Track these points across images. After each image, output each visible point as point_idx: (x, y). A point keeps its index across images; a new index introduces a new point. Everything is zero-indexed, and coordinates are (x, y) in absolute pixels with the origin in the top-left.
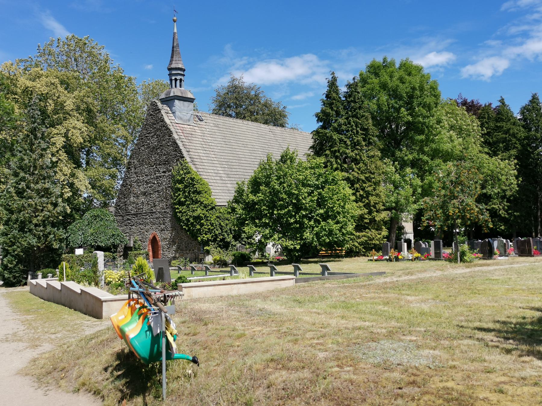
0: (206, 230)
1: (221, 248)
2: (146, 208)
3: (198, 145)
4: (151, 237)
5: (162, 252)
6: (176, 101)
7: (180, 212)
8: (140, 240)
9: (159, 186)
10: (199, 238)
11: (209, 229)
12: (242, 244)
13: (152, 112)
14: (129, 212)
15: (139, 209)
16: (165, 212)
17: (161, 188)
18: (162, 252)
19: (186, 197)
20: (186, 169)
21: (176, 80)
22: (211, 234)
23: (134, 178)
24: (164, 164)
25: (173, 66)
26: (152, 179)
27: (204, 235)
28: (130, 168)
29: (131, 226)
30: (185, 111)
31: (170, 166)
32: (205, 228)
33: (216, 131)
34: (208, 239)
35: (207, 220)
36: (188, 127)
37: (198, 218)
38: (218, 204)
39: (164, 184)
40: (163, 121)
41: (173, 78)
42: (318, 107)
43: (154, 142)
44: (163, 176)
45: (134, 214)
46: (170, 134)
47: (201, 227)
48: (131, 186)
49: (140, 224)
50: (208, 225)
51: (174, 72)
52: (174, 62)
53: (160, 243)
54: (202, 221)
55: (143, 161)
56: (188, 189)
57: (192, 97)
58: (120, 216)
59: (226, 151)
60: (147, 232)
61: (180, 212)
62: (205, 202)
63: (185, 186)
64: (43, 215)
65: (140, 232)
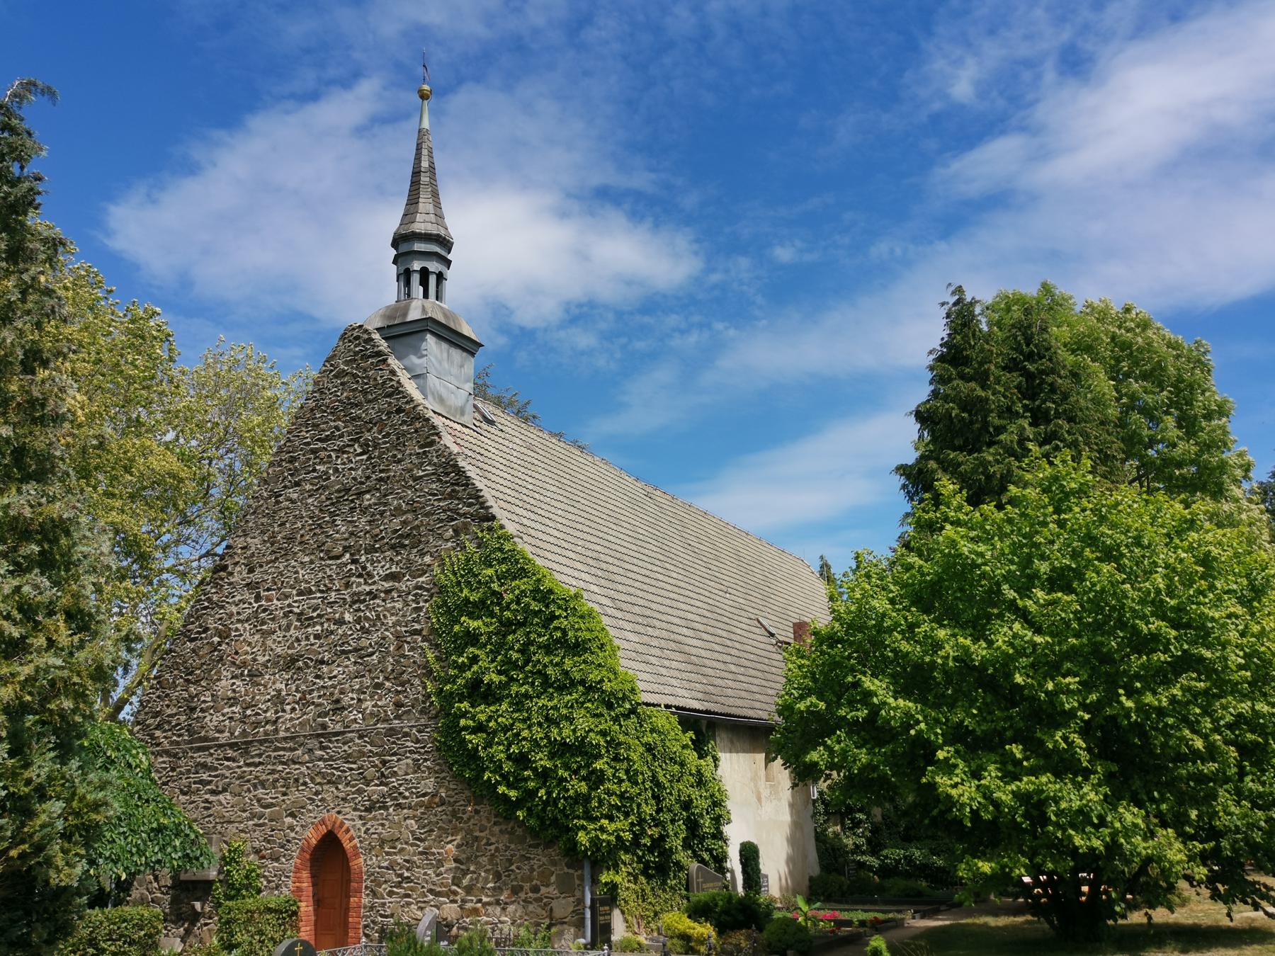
0: (614, 800)
1: (649, 877)
2: (290, 719)
3: (508, 491)
4: (312, 836)
5: (365, 900)
6: (429, 336)
7: (480, 728)
8: (257, 851)
9: (368, 632)
10: (582, 837)
11: (621, 796)
12: (702, 861)
13: (347, 363)
14: (206, 739)
15: (257, 724)
16: (391, 732)
17: (375, 637)
18: (365, 900)
19: (508, 667)
20: (502, 561)
21: (424, 273)
22: (627, 815)
23: (240, 603)
24: (393, 547)
25: (420, 227)
26: (331, 604)
27: (605, 822)
28: (224, 568)
29: (213, 792)
30: (452, 379)
31: (422, 555)
32: (609, 793)
33: (536, 462)
34: (619, 838)
35: (616, 758)
36: (465, 430)
37: (581, 749)
38: (645, 698)
39: (391, 620)
40: (398, 390)
41: (417, 265)
42: (921, 393)
43: (352, 466)
44: (388, 592)
45: (232, 746)
46: (429, 436)
47: (594, 787)
48: (224, 635)
49: (263, 784)
50: (621, 781)
51: (419, 246)
52: (419, 217)
53: (360, 863)
54: (598, 765)
55: (290, 539)
56: (512, 634)
57: (473, 337)
58: (159, 754)
59: (579, 527)
60: (292, 815)
61: (480, 728)
62: (607, 686)
63: (509, 623)
64: (27, 670)
65: (253, 816)
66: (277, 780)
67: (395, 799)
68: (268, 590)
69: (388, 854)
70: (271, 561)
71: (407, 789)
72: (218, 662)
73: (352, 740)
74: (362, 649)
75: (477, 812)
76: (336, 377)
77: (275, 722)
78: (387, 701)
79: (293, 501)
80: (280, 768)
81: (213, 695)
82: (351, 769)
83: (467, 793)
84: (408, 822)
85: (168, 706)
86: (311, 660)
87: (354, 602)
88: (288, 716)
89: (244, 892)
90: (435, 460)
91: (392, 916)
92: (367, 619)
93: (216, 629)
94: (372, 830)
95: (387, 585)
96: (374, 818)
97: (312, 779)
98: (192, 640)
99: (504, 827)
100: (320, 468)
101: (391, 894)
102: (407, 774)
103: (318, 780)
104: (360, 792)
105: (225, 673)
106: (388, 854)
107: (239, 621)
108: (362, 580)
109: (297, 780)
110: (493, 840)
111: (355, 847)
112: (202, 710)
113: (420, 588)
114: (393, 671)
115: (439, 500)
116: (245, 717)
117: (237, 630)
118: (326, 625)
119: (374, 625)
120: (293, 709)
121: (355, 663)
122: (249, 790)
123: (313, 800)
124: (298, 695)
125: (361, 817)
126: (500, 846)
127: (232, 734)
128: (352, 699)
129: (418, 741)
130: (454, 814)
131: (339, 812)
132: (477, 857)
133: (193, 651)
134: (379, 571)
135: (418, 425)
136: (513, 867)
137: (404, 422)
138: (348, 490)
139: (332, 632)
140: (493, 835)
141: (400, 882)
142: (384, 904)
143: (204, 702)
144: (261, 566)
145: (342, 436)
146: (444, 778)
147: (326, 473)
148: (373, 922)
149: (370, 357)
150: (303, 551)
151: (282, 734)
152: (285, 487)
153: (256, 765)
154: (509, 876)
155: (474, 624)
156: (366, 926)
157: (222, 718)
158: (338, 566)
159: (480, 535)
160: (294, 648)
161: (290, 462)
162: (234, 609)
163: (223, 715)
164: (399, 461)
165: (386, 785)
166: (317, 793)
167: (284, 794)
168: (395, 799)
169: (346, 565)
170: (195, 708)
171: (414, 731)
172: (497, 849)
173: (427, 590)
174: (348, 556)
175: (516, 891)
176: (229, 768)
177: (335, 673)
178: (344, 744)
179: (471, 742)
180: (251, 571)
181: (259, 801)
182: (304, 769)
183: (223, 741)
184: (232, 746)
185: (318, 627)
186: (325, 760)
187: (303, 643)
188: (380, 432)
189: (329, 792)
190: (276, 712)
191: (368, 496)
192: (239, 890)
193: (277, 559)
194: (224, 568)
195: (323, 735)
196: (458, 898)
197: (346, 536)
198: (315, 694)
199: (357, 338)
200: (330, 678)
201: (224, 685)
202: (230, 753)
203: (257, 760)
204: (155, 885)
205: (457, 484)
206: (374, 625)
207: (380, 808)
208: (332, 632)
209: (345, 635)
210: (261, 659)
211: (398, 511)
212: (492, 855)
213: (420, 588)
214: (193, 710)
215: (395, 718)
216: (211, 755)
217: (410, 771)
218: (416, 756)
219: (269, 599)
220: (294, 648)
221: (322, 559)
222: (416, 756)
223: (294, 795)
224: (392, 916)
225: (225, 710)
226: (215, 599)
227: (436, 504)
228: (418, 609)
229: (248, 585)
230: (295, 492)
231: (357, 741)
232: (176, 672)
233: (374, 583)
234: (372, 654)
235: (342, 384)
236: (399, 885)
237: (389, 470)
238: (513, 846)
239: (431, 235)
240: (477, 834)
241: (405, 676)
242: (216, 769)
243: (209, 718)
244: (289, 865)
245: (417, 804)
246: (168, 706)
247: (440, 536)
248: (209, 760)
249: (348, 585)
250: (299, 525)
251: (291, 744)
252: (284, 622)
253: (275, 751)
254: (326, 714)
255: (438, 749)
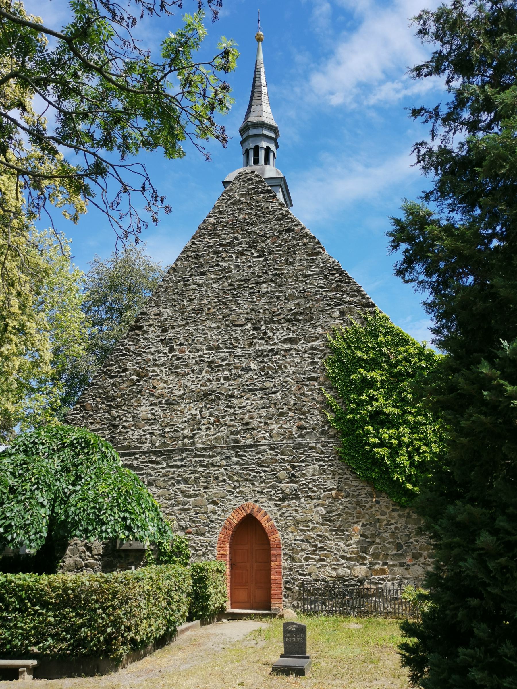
5: (285, 564)
8: (183, 529)
14: (128, 448)
15: (175, 439)
16: (299, 446)
24: (289, 321)
31: (315, 327)
39: (291, 370)
44: (287, 350)
45: (155, 453)
46: (315, 250)
49: (186, 481)
53: (278, 537)
55: (199, 310)
60: (214, 503)
65: (177, 504)
66: (199, 478)
67: (306, 492)
68: (181, 344)
69: (302, 530)
70: (182, 325)
71: (315, 486)
72: (138, 393)
73: (265, 451)
74: (267, 388)
75: (377, 502)
76: (232, 204)
77: (192, 437)
78: (291, 426)
79: (199, 285)
80: (201, 469)
81: (133, 417)
82: (265, 471)
83: (368, 489)
84: (319, 508)
85: (92, 423)
86: (223, 394)
87: (258, 357)
88: (204, 433)
89: (174, 558)
90: (322, 265)
91: (310, 574)
92: (270, 368)
93: (135, 370)
94: (287, 514)
95: (287, 346)
96: (289, 506)
97: (230, 478)
98: (111, 377)
99: (401, 513)
100: (224, 264)
101: (307, 559)
102: (314, 475)
103: (236, 478)
104: (273, 487)
105: (144, 401)
106: (302, 530)
107: (155, 365)
108: (263, 342)
109: (217, 478)
110: (393, 521)
111: (272, 526)
112: (124, 427)
113: (315, 349)
114: (295, 404)
115: (327, 291)
116: (165, 433)
117: (154, 371)
118: (234, 371)
119: (276, 373)
120: (209, 429)
121: (262, 398)
122: (173, 485)
123: (232, 493)
124: (212, 419)
125: (276, 505)
126: (399, 525)
127: (153, 444)
128: (260, 423)
129: (322, 453)
130: (358, 503)
131: (256, 501)
132: (379, 533)
133: (114, 385)
134: (279, 335)
135: (306, 241)
136: (411, 540)
137: (293, 238)
138: (247, 281)
139: (240, 376)
140: (392, 518)
141: (314, 551)
142: (302, 566)
143: (126, 421)
144: (173, 328)
145: (241, 243)
146: (348, 479)
147: (229, 268)
148: (293, 579)
149: (261, 193)
150: (211, 320)
151: (199, 446)
152: (192, 275)
153: (178, 467)
154: (409, 546)
155: (370, 375)
156: (286, 582)
157: (143, 433)
158: (242, 331)
159: (363, 316)
160: (206, 385)
161: (196, 258)
162: (150, 357)
163: (144, 431)
164: (291, 264)
165: (296, 482)
166: (235, 487)
167: (206, 488)
168: (306, 492)
169: (249, 331)
170: (118, 426)
171: (319, 445)
172: (396, 528)
173: (321, 351)
174: (249, 325)
175: (416, 557)
176: (154, 469)
177: (243, 404)
178: (258, 453)
179: (378, 453)
180: (164, 331)
181: (182, 492)
182: (222, 470)
183: (146, 450)
184: (155, 453)
185: (226, 372)
186: (241, 465)
187: (214, 383)
188: (273, 243)
189: (247, 487)
190: (193, 430)
191: (265, 286)
192: (171, 557)
193: (188, 324)
194: (140, 328)
195: (236, 446)
196: (367, 562)
197: (248, 311)
198: (227, 418)
199: (250, 180)
200: (240, 408)
201: (144, 411)
202: (153, 458)
203: (179, 463)
204: (88, 553)
205: (341, 282)
206: (276, 373)
207: (292, 499)
208: (240, 376)
209: (252, 378)
210: (177, 393)
211: (292, 296)
212: (393, 532)
213: (315, 349)
214: (116, 426)
215: (299, 437)
216: (137, 459)
217: (316, 473)
218: (322, 463)
219: (181, 351)
220: (206, 385)
221: (227, 326)
222: (322, 463)
223: (215, 490)
224: (310, 574)
225: (146, 428)
226: (132, 348)
227: (324, 293)
228: (314, 363)
229: (162, 341)
230: (201, 279)
231: (269, 451)
232: (98, 399)
233: (275, 344)
234: (277, 392)
235: (238, 209)
236: (314, 553)
237: (282, 269)
238: (410, 526)
239: (273, 126)
240: (379, 517)
241: (306, 409)
242: (142, 469)
243: (131, 433)
244: (214, 539)
245: (325, 496)
246: (92, 423)
247: (330, 315)
248: (135, 463)
249: (251, 344)
250: (206, 301)
251: (210, 453)
252: (196, 368)
253: (195, 457)
254: (238, 433)
255: (340, 458)
